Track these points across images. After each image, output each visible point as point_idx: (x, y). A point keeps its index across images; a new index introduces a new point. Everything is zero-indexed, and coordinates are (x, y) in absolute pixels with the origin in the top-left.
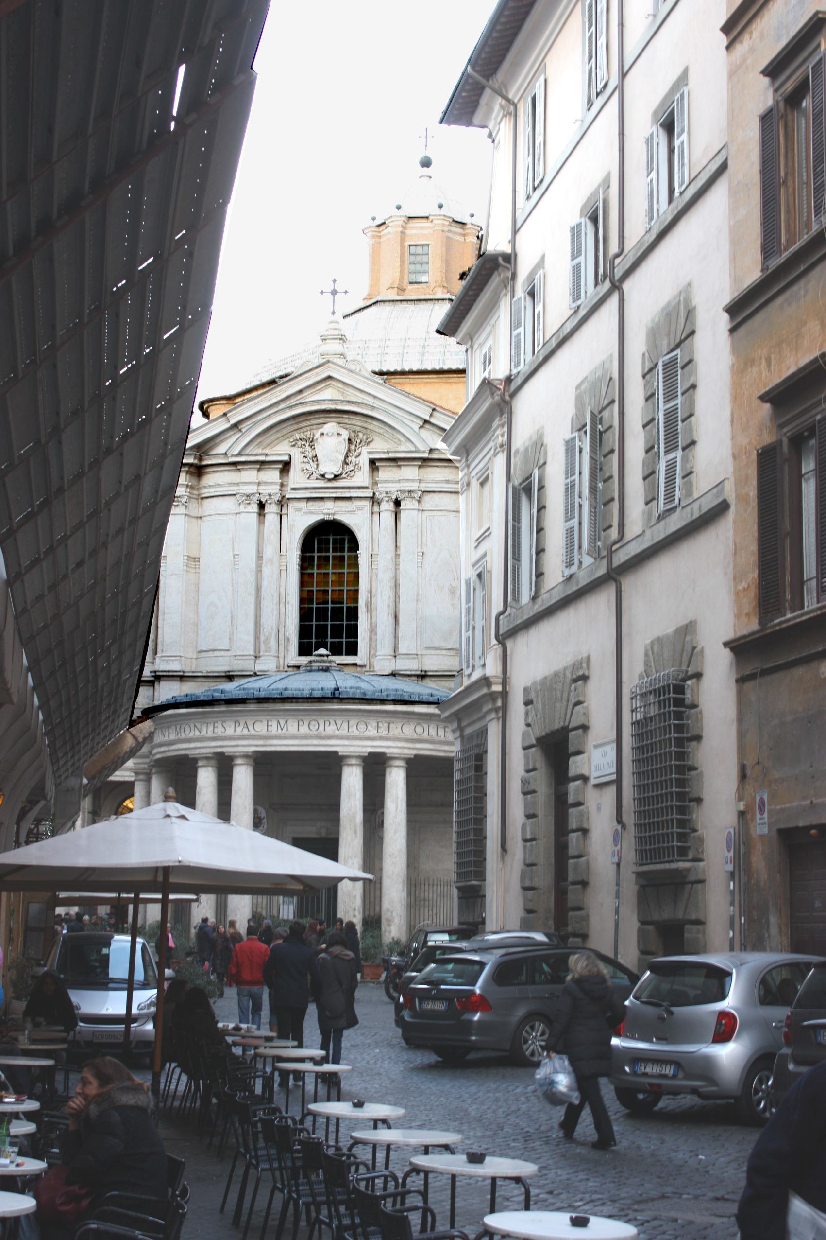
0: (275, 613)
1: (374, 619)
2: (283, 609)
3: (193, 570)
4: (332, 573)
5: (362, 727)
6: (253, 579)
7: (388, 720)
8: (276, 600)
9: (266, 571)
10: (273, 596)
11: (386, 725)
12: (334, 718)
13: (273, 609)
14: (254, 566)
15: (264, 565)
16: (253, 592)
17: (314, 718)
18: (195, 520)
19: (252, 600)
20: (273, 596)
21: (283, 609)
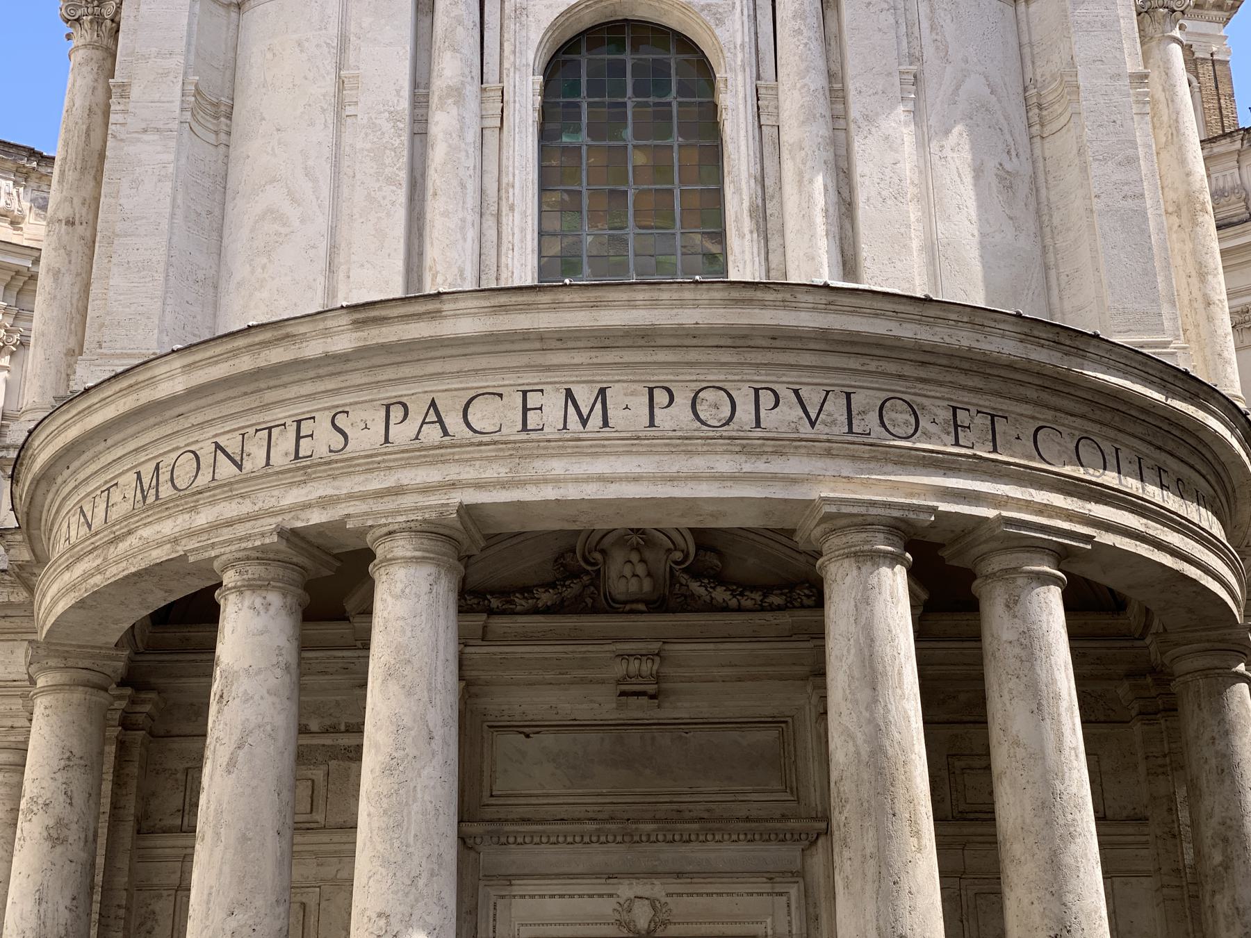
0: (471, 234)
1: (775, 259)
2: (491, 234)
3: (211, 138)
4: (634, 146)
5: (899, 417)
6: (402, 141)
7: (987, 402)
8: (472, 200)
9: (442, 121)
10: (463, 186)
11: (982, 422)
12: (792, 376)
13: (463, 220)
14: (404, 104)
15: (434, 100)
16: (403, 175)
17: (715, 376)
18: (222, 11)
19: (402, 196)
20: (463, 186)
21: (491, 234)
